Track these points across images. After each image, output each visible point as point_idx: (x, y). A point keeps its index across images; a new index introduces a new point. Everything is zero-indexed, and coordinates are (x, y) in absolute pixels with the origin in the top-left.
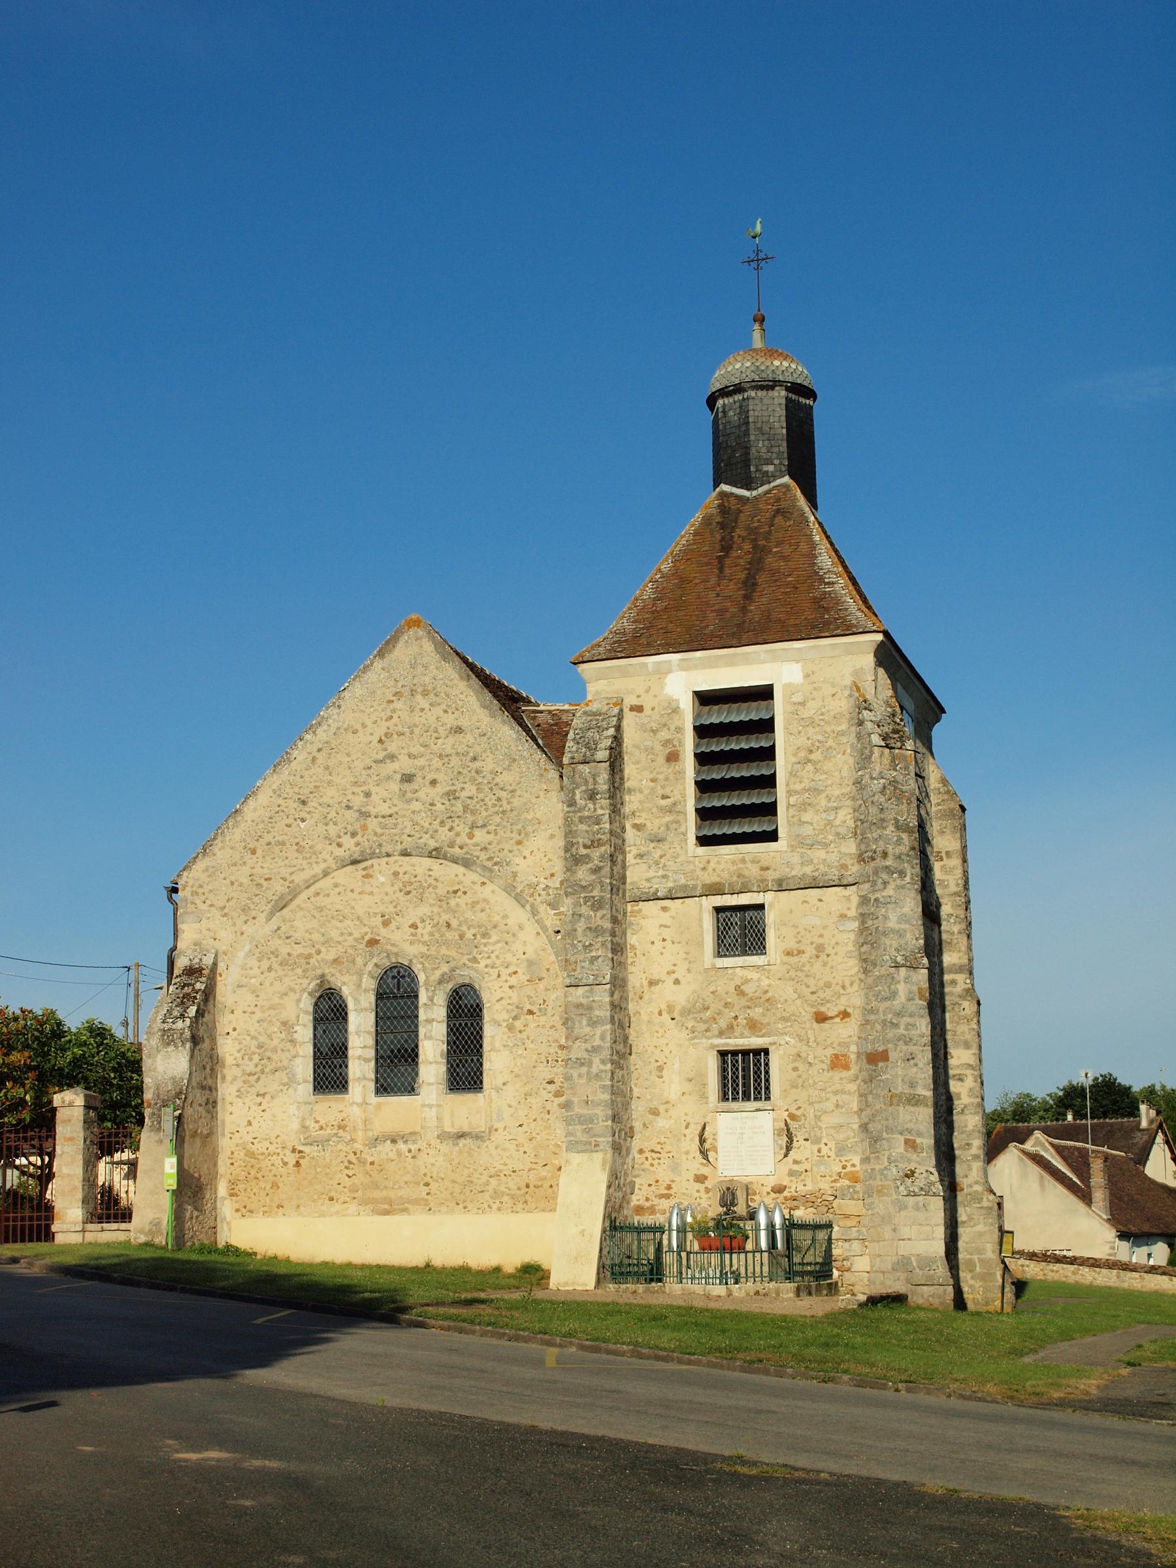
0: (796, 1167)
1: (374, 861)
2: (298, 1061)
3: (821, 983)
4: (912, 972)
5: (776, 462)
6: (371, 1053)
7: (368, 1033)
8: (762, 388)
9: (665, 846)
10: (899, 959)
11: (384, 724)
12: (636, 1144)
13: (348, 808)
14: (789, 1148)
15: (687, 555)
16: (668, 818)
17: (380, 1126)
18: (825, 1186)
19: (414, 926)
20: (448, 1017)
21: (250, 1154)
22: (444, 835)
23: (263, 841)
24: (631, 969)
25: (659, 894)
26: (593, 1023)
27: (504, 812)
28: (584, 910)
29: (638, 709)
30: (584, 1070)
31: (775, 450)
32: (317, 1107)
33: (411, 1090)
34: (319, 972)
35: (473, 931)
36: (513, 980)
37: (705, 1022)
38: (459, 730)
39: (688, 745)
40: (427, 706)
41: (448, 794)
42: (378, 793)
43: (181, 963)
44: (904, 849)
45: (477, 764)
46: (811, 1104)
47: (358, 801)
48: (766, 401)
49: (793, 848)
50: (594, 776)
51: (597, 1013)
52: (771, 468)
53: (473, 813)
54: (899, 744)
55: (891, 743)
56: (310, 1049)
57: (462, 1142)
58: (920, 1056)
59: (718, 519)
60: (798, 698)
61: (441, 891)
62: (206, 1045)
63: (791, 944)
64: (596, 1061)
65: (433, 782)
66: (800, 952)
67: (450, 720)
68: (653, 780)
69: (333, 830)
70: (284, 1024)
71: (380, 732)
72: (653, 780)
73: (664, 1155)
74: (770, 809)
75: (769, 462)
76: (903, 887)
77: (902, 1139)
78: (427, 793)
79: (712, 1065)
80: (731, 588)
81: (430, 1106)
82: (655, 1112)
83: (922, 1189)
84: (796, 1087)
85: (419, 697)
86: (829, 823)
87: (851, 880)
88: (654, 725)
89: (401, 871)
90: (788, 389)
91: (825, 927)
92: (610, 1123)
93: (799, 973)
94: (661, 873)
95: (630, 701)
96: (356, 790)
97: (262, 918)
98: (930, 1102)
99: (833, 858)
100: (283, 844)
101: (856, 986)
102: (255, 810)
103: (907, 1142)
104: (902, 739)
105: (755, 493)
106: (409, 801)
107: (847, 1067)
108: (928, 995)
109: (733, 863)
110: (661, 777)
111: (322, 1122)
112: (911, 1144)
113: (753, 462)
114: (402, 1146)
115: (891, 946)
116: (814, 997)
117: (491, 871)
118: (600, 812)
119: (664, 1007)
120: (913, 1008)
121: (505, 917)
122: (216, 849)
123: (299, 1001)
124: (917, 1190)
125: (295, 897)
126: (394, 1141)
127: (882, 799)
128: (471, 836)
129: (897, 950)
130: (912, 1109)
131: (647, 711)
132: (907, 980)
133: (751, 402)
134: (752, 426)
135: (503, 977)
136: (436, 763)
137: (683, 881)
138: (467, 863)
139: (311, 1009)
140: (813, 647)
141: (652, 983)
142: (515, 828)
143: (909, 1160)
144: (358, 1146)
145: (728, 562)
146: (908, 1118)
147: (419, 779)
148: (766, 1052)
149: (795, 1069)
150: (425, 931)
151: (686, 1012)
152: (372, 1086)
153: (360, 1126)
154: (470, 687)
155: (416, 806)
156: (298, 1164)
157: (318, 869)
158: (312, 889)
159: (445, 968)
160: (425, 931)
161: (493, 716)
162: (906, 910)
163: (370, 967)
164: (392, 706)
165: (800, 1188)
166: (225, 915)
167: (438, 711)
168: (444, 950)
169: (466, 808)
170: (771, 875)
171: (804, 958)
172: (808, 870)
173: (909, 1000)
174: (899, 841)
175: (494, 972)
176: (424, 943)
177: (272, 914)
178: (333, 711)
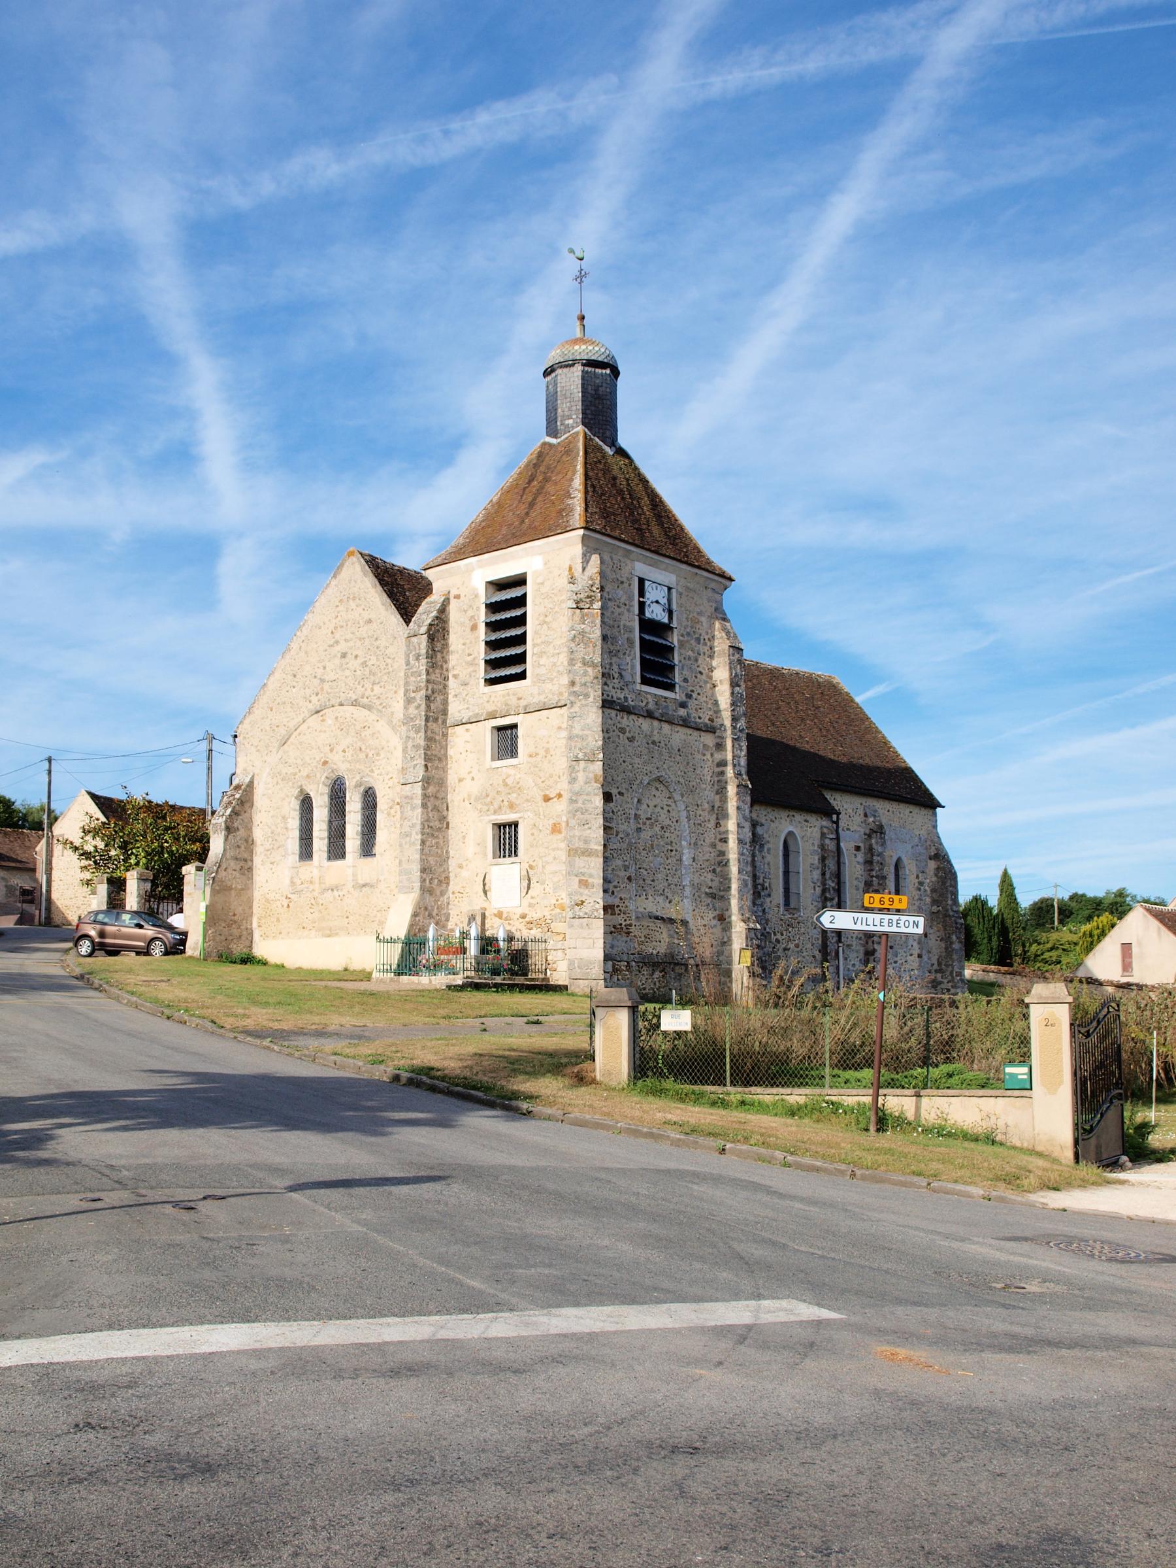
0: (532, 901)
1: (326, 710)
2: (289, 841)
3: (547, 775)
4: (589, 764)
5: (574, 417)
6: (326, 834)
7: (323, 821)
8: (567, 366)
9: (468, 688)
10: (581, 756)
11: (334, 621)
12: (451, 888)
13: (315, 677)
14: (529, 888)
15: (507, 492)
16: (471, 669)
17: (330, 880)
18: (547, 914)
19: (344, 751)
20: (363, 808)
21: (267, 901)
22: (360, 690)
23: (276, 702)
24: (449, 772)
25: (464, 721)
26: (413, 809)
27: (389, 673)
28: (412, 734)
29: (457, 597)
30: (408, 839)
31: (574, 408)
32: (302, 870)
33: (329, 859)
34: (299, 784)
35: (373, 752)
36: (390, 784)
37: (487, 805)
38: (370, 621)
39: (482, 616)
40: (354, 607)
41: (362, 664)
42: (330, 666)
43: (235, 783)
44: (588, 679)
45: (378, 642)
46: (541, 857)
47: (320, 672)
48: (568, 375)
49: (534, 683)
50: (419, 644)
51: (415, 801)
52: (571, 421)
53: (374, 675)
54: (587, 606)
55: (581, 605)
56: (297, 834)
57: (364, 889)
58: (593, 822)
59: (534, 462)
60: (540, 580)
61: (358, 727)
62: (242, 833)
63: (532, 750)
64: (414, 833)
65: (356, 657)
66: (537, 754)
67: (366, 616)
68: (464, 644)
69: (308, 691)
70: (283, 818)
71: (331, 627)
72: (464, 644)
73: (465, 895)
74: (521, 659)
75: (569, 417)
76: (586, 705)
77: (577, 880)
78: (354, 664)
79: (489, 833)
80: (523, 508)
81: (349, 867)
82: (461, 867)
83: (586, 913)
84: (532, 846)
85: (351, 601)
86: (555, 664)
87: (563, 704)
88: (465, 607)
89: (339, 715)
90: (584, 365)
91: (550, 736)
92: (419, 874)
93: (537, 769)
94: (466, 706)
95: (453, 592)
96: (320, 665)
97: (274, 750)
98: (601, 854)
99: (555, 688)
100: (284, 703)
101: (565, 777)
102: (273, 682)
103: (580, 881)
104: (592, 603)
105: (559, 440)
106: (343, 670)
107: (560, 832)
108: (601, 779)
109: (504, 696)
110: (468, 641)
111: (303, 879)
112: (584, 883)
113: (559, 419)
114: (336, 893)
115: (575, 747)
116: (543, 785)
117: (381, 712)
118: (421, 668)
119: (466, 796)
120: (590, 789)
121: (388, 742)
122: (255, 709)
123: (290, 803)
124: (582, 914)
125: (290, 736)
126: (332, 890)
127: (573, 645)
128: (372, 690)
129: (580, 749)
130: (586, 858)
131: (462, 598)
132: (584, 770)
133: (559, 378)
134: (559, 393)
135: (386, 781)
136: (358, 643)
137: (477, 711)
138: (369, 707)
139: (298, 807)
140: (557, 541)
141: (460, 780)
142: (396, 682)
143: (581, 894)
144: (316, 894)
145: (527, 490)
146: (582, 865)
147: (349, 655)
148: (516, 825)
149: (533, 834)
150: (349, 753)
151: (477, 799)
152: (325, 855)
153: (317, 881)
154: (376, 592)
155: (347, 673)
156: (288, 906)
157: (300, 719)
158: (298, 731)
159: (358, 777)
160: (349, 753)
161: (387, 610)
162: (589, 721)
163: (323, 778)
164: (338, 609)
165: (534, 915)
166: (258, 751)
167: (360, 610)
168: (358, 766)
169: (370, 671)
170: (523, 703)
171: (539, 758)
172: (542, 698)
173: (586, 783)
174: (585, 674)
175: (381, 778)
176: (349, 762)
177: (279, 748)
178: (311, 615)
